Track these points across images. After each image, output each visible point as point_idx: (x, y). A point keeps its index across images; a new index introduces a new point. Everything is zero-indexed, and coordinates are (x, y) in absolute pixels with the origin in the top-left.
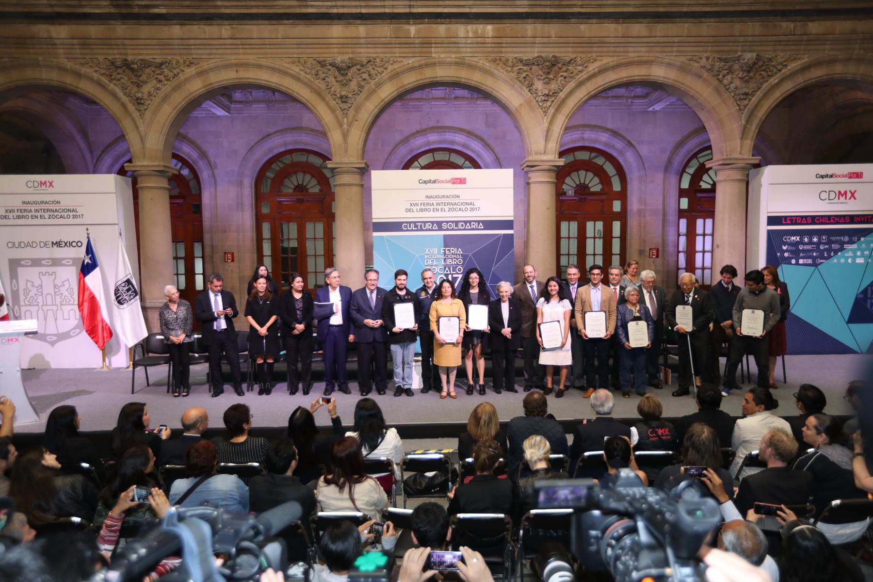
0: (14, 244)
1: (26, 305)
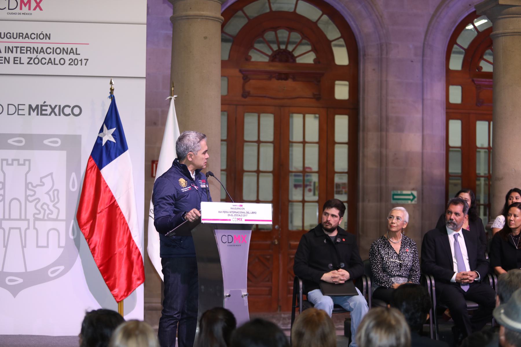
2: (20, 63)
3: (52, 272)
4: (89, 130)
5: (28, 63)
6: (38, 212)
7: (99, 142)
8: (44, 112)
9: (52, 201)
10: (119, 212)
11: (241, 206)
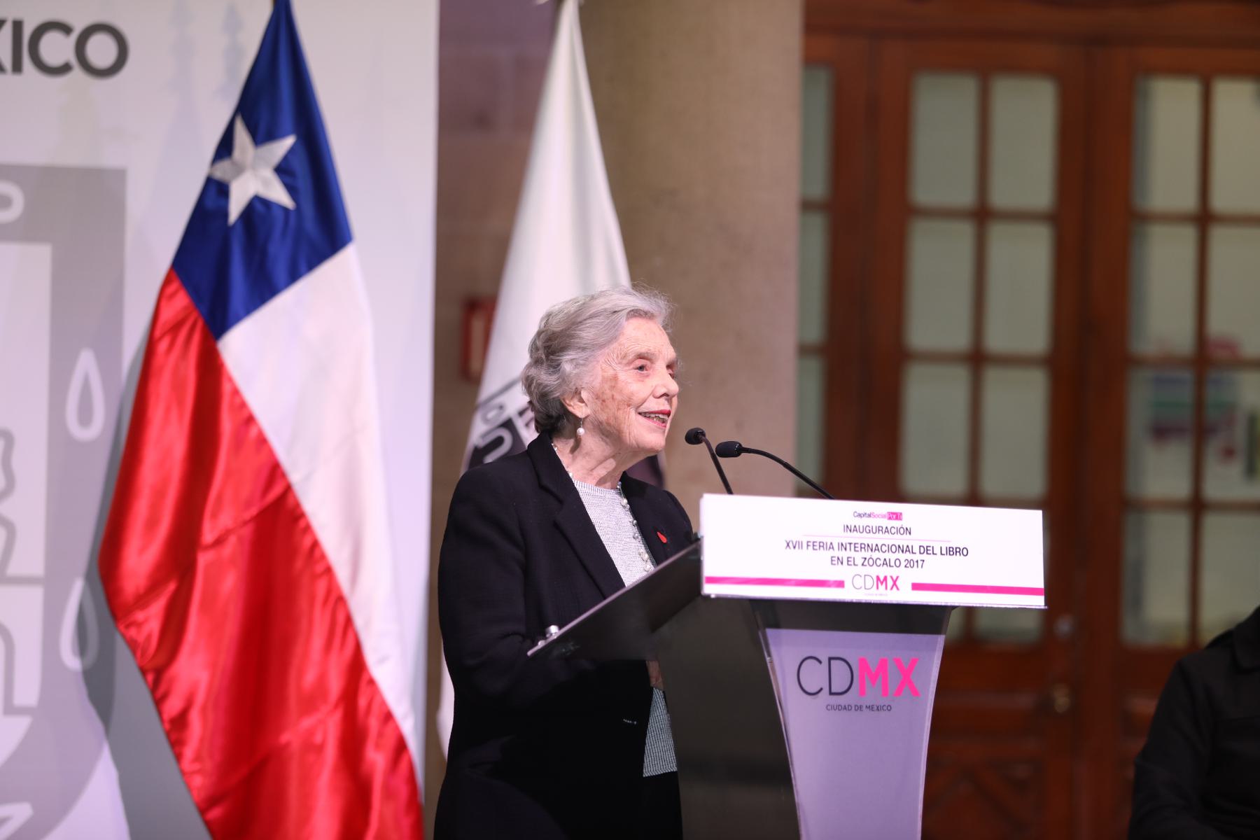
4: (163, 148)
7: (211, 203)
10: (307, 542)
11: (897, 516)
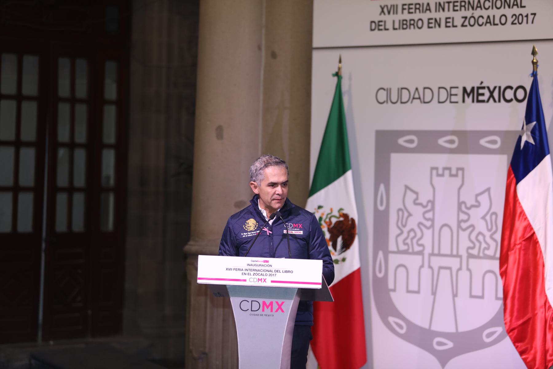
0: (389, 91)
1: (399, 252)
2: (454, 26)
3: (489, 335)
5: (463, 25)
6: (471, 245)
8: (481, 98)
9: (489, 230)
11: (267, 262)
